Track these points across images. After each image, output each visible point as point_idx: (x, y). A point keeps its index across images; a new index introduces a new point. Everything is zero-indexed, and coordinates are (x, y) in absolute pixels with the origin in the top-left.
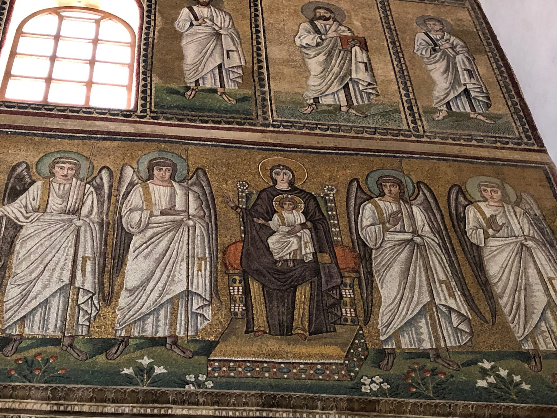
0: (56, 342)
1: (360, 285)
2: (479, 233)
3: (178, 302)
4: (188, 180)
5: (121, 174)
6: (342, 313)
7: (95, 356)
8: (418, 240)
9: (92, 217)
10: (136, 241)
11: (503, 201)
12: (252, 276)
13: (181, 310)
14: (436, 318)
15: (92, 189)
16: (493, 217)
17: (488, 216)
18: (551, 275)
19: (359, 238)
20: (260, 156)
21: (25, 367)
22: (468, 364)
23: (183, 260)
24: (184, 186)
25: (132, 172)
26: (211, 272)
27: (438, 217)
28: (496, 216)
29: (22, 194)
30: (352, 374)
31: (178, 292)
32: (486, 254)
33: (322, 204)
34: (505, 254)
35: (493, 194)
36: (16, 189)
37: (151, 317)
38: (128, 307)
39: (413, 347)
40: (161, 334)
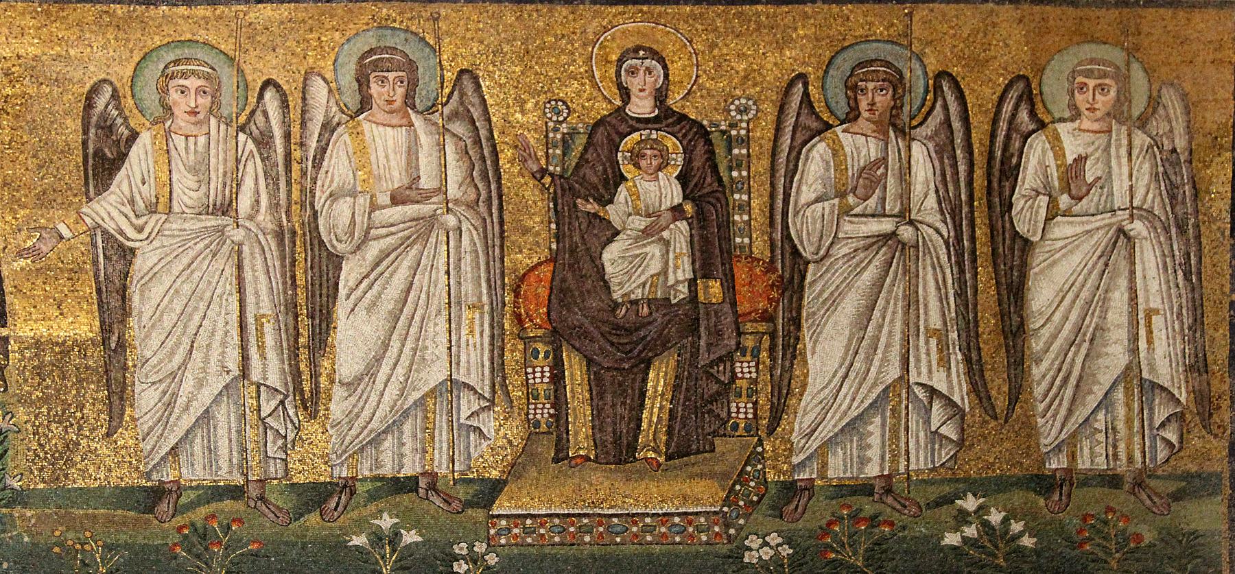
0: (235, 492)
1: (772, 349)
2: (1039, 206)
3: (435, 404)
4: (444, 105)
5: (304, 99)
6: (729, 413)
7: (302, 515)
8: (906, 233)
9: (260, 218)
10: (349, 274)
11: (1114, 117)
12: (568, 343)
13: (441, 421)
14: (904, 412)
15: (251, 145)
16: (1081, 160)
17: (1070, 160)
18: (1155, 303)
19: (787, 237)
20: (595, 23)
21: (195, 539)
22: (938, 504)
23: (439, 312)
24: (436, 124)
25: (325, 91)
26: (492, 337)
27: (962, 168)
28: (1086, 158)
29: (119, 169)
30: (732, 531)
31: (432, 384)
32: (1038, 260)
33: (720, 151)
34: (1076, 258)
35: (1098, 96)
36: (105, 154)
37: (390, 437)
38: (347, 420)
39: (848, 475)
40: (407, 471)
